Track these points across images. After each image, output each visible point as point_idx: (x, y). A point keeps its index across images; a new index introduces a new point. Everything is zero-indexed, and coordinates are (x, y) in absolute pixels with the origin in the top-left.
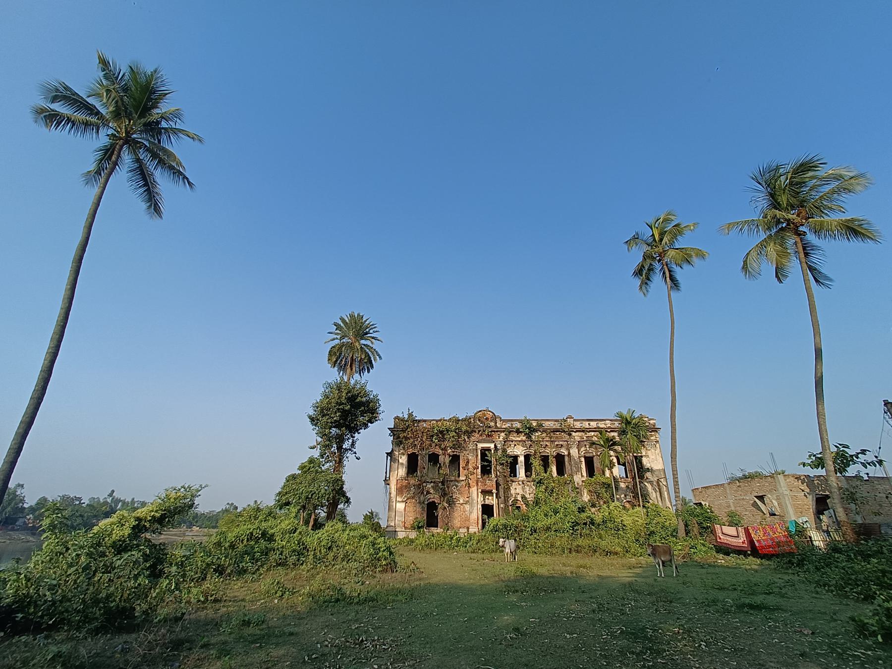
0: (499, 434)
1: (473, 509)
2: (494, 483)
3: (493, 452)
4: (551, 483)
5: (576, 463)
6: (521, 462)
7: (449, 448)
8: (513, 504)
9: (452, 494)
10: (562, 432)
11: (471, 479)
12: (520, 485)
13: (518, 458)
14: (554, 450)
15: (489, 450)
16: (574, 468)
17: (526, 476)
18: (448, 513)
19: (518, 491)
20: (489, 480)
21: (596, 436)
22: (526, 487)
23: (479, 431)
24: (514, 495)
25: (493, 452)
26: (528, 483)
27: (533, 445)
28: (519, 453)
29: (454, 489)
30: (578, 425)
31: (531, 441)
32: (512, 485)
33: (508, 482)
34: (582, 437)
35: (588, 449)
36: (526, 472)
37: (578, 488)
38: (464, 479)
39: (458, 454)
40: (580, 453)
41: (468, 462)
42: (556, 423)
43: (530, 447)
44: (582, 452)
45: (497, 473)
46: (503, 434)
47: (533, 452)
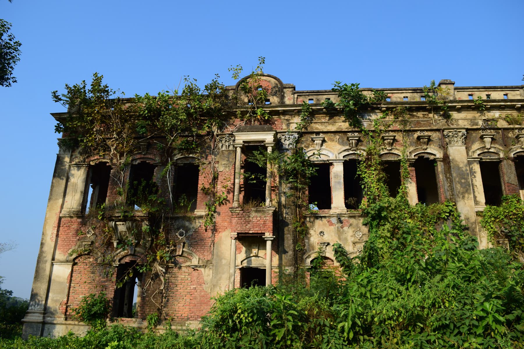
0: (287, 120)
1: (220, 279)
2: (269, 219)
3: (270, 150)
4: (406, 218)
5: (463, 175)
6: (336, 176)
7: (176, 152)
8: (315, 268)
9: (175, 246)
10: (430, 111)
11: (219, 214)
12: (331, 224)
13: (331, 167)
14: (412, 149)
15: (260, 146)
16: (458, 186)
17: (348, 206)
18: (162, 288)
19: (326, 238)
20: (257, 211)
21: (504, 119)
22: (346, 228)
23: (243, 114)
24: (317, 248)
25: (270, 150)
26: (352, 221)
27: (365, 140)
28: (332, 157)
29: (181, 234)
30: (464, 96)
31: (359, 132)
32: (313, 226)
33: (305, 217)
34: (473, 121)
35: (488, 146)
36: (346, 197)
37: (467, 229)
38: (203, 213)
39: (196, 162)
40: (470, 154)
41: (215, 179)
42: (415, 94)
43: (357, 145)
44: (474, 152)
45: (280, 199)
46: (297, 120)
47: (365, 154)
